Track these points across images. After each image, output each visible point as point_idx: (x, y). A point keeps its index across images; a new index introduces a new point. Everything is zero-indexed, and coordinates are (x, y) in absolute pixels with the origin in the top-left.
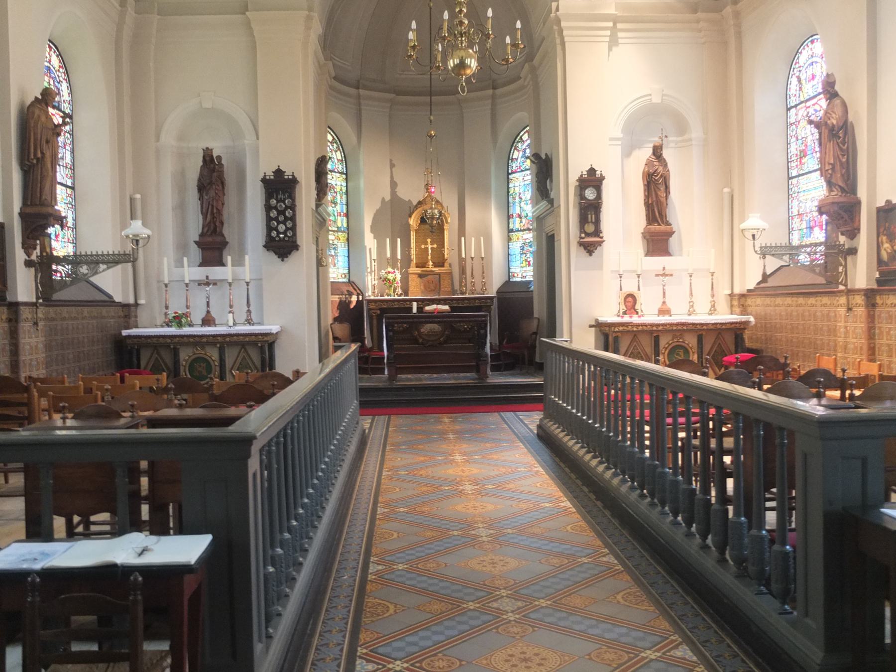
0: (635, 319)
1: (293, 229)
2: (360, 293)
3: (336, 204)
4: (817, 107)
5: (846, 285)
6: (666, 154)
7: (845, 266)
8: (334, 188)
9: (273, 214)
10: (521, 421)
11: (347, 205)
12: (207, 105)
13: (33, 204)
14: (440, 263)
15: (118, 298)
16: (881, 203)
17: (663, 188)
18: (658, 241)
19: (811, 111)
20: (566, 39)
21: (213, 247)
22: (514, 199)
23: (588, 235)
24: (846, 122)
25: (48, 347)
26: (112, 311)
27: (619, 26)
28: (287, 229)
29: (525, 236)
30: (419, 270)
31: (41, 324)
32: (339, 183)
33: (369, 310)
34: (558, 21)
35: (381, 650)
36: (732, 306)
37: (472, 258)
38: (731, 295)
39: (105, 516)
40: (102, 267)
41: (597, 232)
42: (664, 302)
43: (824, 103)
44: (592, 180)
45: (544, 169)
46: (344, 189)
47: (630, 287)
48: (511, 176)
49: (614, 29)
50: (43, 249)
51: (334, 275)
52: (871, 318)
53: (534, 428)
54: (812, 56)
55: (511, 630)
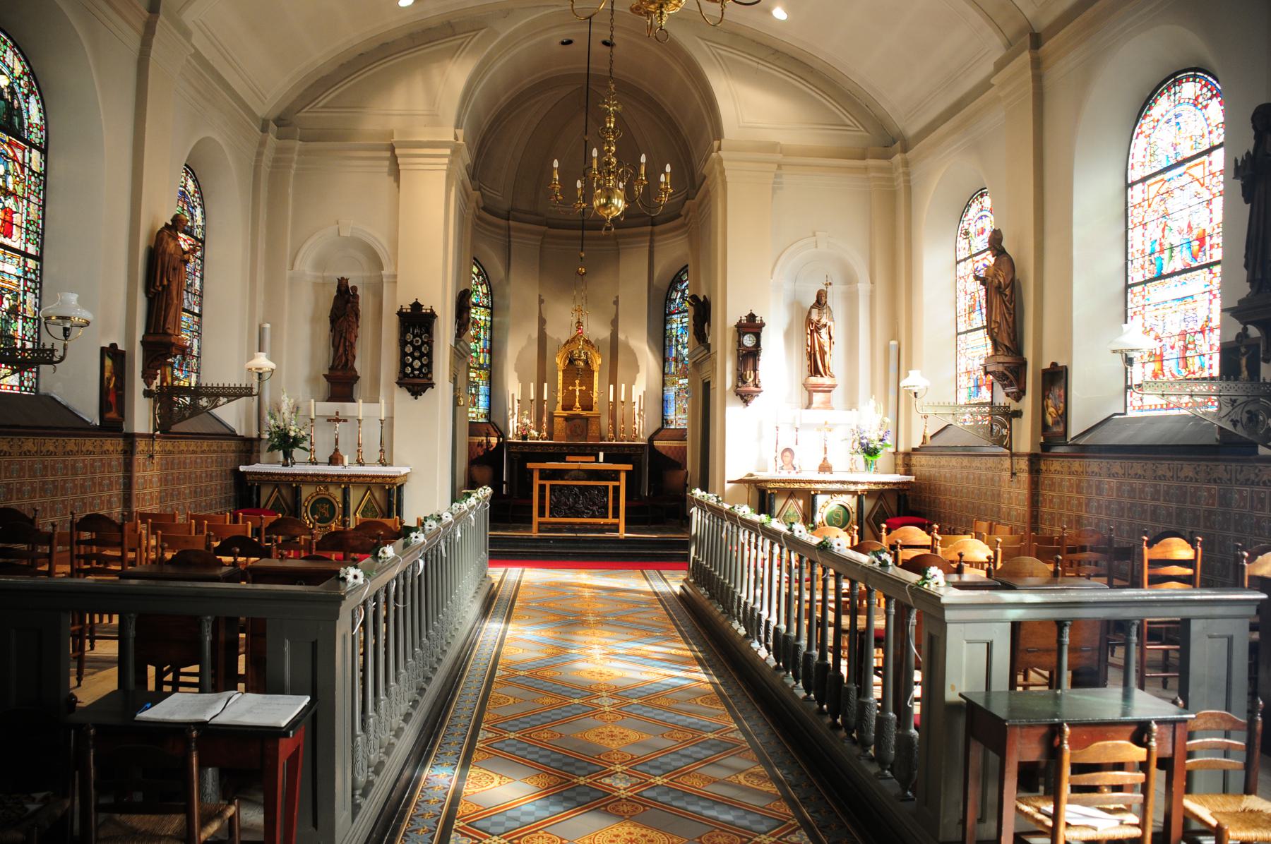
1: (429, 365)
2: (502, 434)
3: (479, 339)
4: (987, 263)
5: (1010, 449)
7: (1010, 429)
9: (409, 349)
11: (491, 341)
12: (346, 233)
13: (156, 333)
14: (588, 406)
15: (238, 433)
16: (1047, 365)
19: (980, 265)
21: (341, 382)
24: (1013, 280)
25: (164, 480)
26: (233, 445)
28: (423, 365)
30: (565, 413)
31: (157, 457)
34: (720, 161)
35: (478, 824)
36: (896, 465)
38: (896, 453)
39: (195, 668)
40: (223, 400)
43: (990, 259)
44: (752, 326)
45: (702, 312)
46: (488, 324)
50: (162, 382)
52: (1035, 485)
55: (621, 809)
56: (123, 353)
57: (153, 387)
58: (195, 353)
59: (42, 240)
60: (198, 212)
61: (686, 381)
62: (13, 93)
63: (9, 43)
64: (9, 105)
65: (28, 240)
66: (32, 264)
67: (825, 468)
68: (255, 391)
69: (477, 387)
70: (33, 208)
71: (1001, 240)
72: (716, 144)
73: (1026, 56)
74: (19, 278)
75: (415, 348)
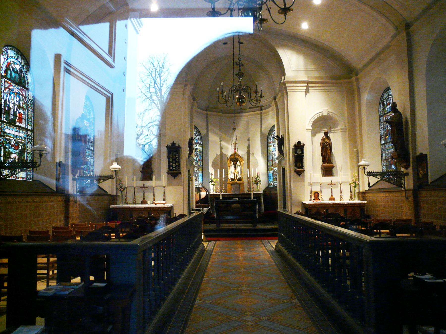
0: (319, 202)
1: (179, 166)
2: (207, 191)
3: (198, 156)
6: (331, 135)
10: (270, 243)
11: (202, 156)
15: (110, 193)
17: (329, 149)
18: (328, 170)
20: (288, 91)
23: (298, 168)
26: (107, 198)
27: (310, 85)
28: (176, 166)
29: (274, 169)
30: (231, 182)
32: (199, 148)
38: (359, 193)
41: (302, 166)
42: (332, 195)
44: (299, 147)
45: (281, 142)
46: (201, 150)
47: (316, 188)
49: (307, 87)
50: (80, 174)
51: (197, 184)
53: (274, 246)
54: (389, 96)
56: (64, 165)
57: (76, 177)
58: (92, 164)
59: (34, 124)
60: (92, 113)
61: (276, 168)
62: (21, 71)
63: (20, 53)
64: (20, 76)
65: (28, 124)
66: (30, 133)
67: (332, 199)
68: (114, 176)
70: (30, 113)
71: (396, 106)
72: (283, 78)
73: (404, 33)
74: (25, 138)
75: (173, 159)
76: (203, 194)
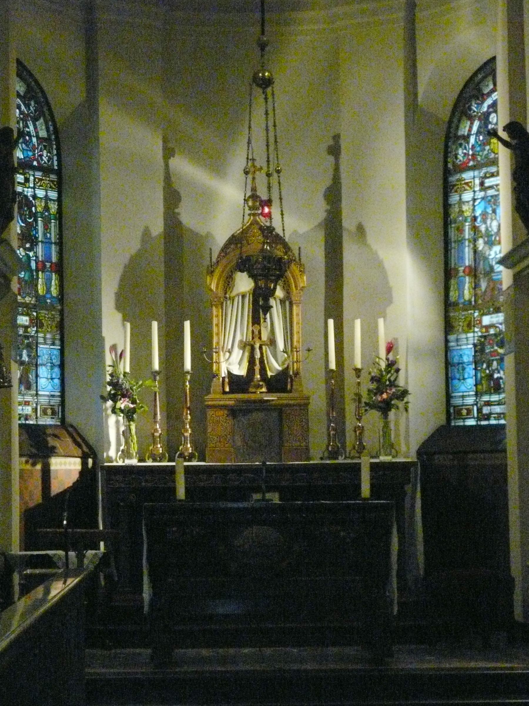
2: (89, 451)
3: (34, 242)
8: (29, 205)
11: (60, 244)
22: (460, 230)
29: (486, 320)
30: (231, 400)
32: (41, 193)
33: (109, 494)
37: (358, 371)
46: (53, 207)
48: (453, 179)
51: (28, 410)
61: (498, 318)
69: (33, 347)
76: (66, 468)
